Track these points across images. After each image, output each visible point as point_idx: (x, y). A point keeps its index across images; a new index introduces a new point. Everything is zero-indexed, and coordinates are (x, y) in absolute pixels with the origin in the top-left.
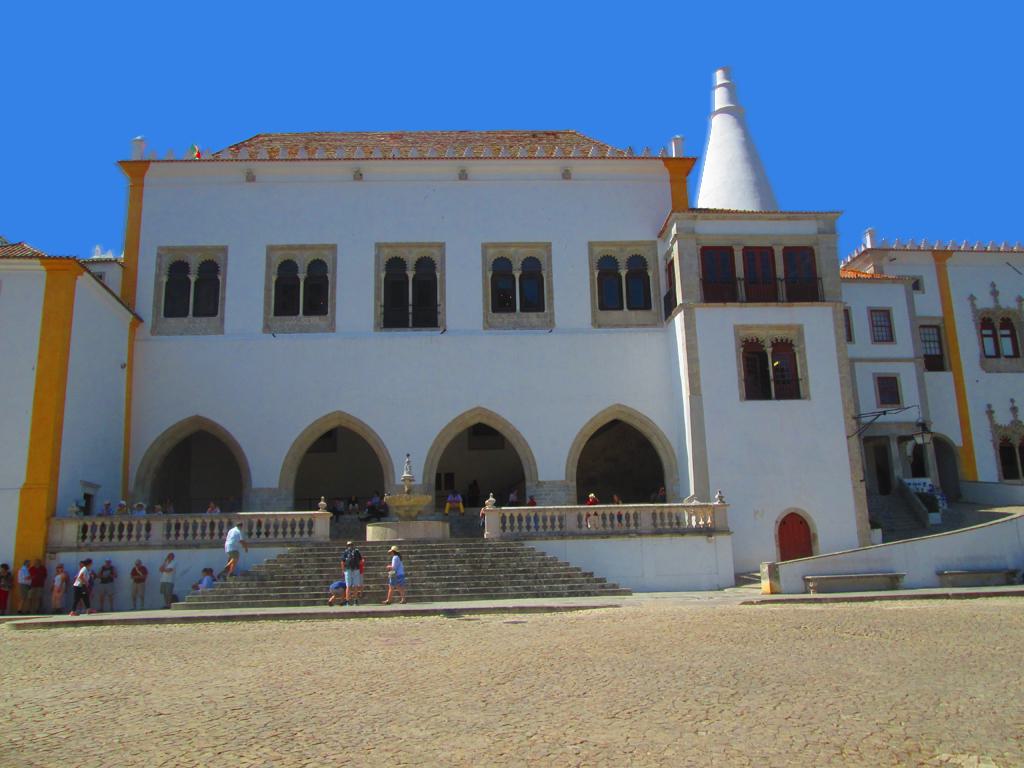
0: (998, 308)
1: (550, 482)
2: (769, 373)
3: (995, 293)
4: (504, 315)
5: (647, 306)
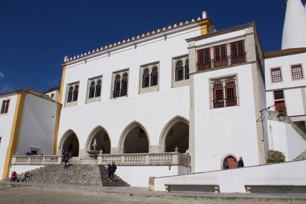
1: (154, 146)
2: (225, 95)
4: (145, 88)
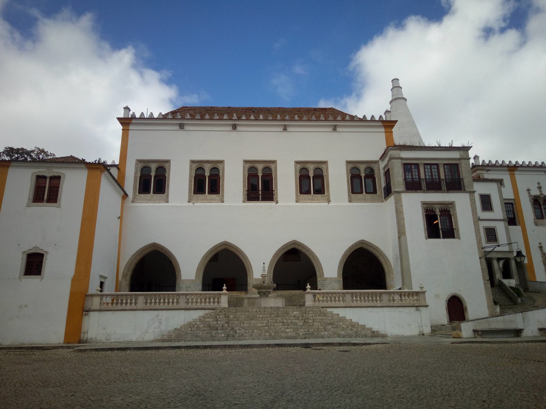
0: (542, 194)
3: (540, 188)
5: (375, 192)
